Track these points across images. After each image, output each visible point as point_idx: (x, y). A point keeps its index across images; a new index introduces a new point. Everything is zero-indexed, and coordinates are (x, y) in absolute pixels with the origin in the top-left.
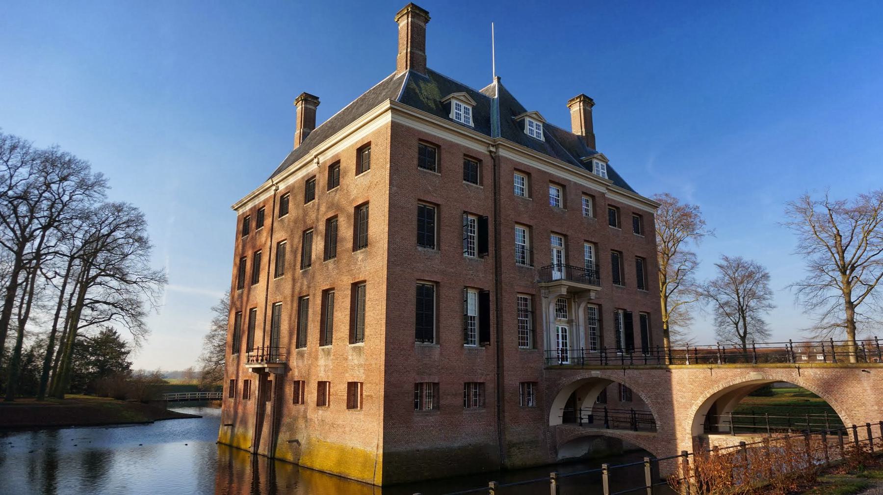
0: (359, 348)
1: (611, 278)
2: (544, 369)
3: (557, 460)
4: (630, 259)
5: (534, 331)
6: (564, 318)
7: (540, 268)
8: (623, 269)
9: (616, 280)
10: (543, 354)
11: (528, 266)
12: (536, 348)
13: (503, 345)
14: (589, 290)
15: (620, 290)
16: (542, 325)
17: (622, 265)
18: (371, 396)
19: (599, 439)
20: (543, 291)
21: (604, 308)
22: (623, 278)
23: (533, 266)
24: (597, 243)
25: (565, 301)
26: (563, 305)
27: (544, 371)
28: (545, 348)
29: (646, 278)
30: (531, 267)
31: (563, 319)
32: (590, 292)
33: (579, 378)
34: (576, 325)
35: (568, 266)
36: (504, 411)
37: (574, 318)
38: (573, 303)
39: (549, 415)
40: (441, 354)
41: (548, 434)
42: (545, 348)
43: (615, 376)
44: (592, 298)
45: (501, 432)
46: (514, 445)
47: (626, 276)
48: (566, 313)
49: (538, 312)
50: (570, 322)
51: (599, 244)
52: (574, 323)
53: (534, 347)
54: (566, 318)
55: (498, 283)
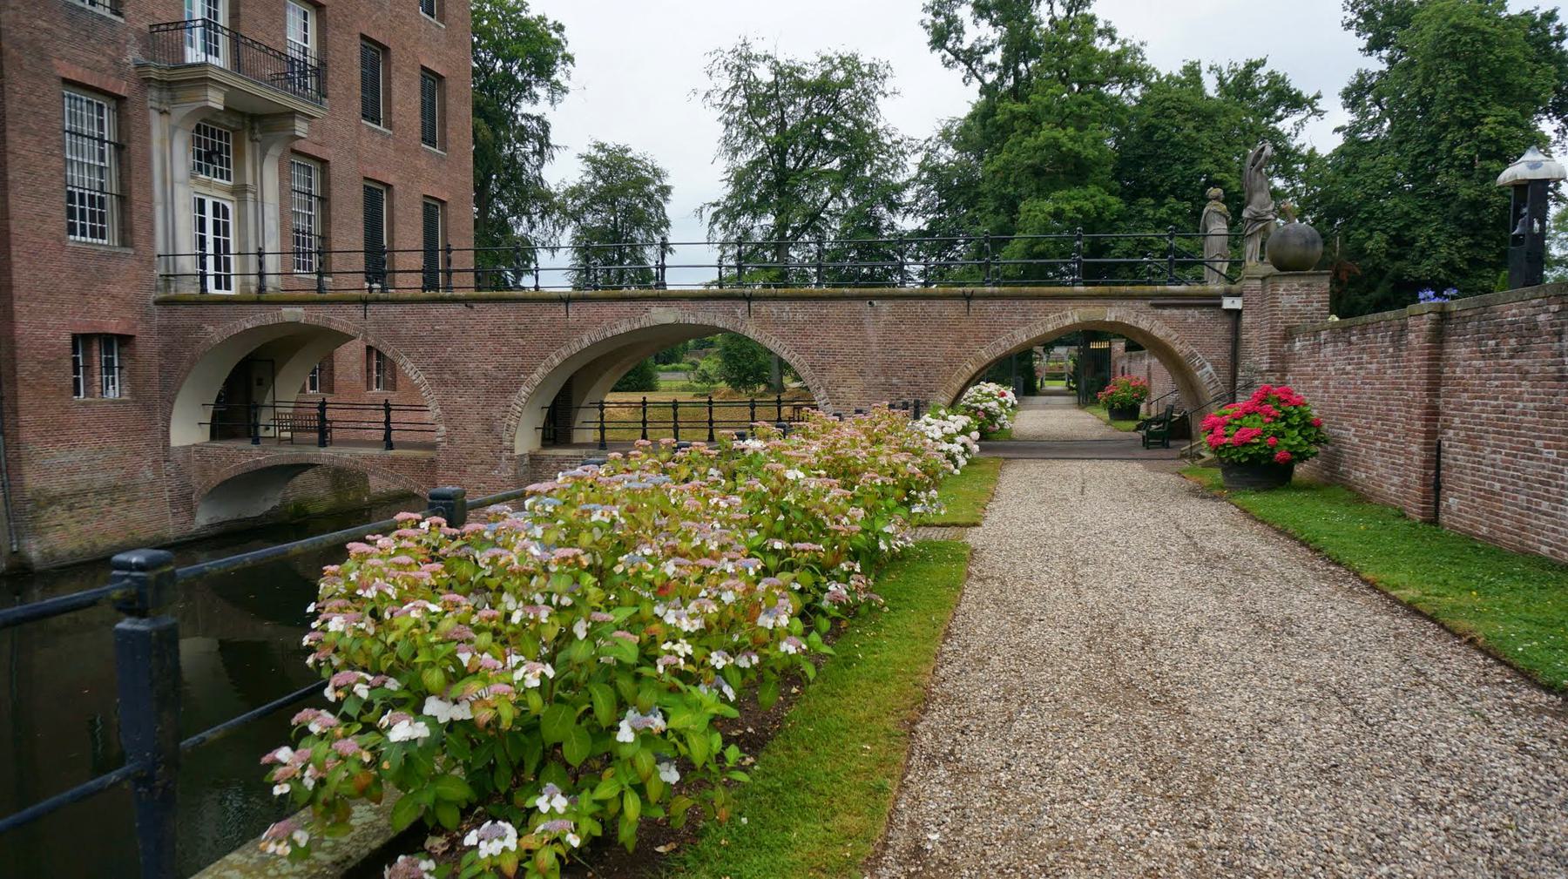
1: (357, 104)
2: (157, 303)
3: (194, 528)
4: (407, 70)
5: (123, 199)
6: (222, 178)
7: (144, 25)
8: (388, 92)
9: (371, 112)
10: (151, 262)
11: (107, 13)
12: (132, 246)
13: (8, 225)
14: (292, 114)
15: (378, 138)
16: (148, 186)
17: (388, 79)
19: (310, 473)
21: (335, 171)
22: (389, 113)
23: (120, 14)
24: (324, 6)
25: (227, 134)
26: (213, 143)
27: (156, 309)
28: (160, 248)
29: (443, 126)
30: (114, 17)
31: (218, 180)
32: (294, 118)
33: (249, 326)
34: (256, 200)
35: (236, 38)
37: (249, 181)
38: (248, 146)
39: (168, 421)
41: (170, 467)
43: (343, 319)
44: (297, 133)
46: (53, 501)
47: (396, 108)
48: (228, 166)
49: (135, 146)
50: (239, 191)
51: (328, 9)
52: (250, 196)
53: (124, 242)
54: (228, 179)
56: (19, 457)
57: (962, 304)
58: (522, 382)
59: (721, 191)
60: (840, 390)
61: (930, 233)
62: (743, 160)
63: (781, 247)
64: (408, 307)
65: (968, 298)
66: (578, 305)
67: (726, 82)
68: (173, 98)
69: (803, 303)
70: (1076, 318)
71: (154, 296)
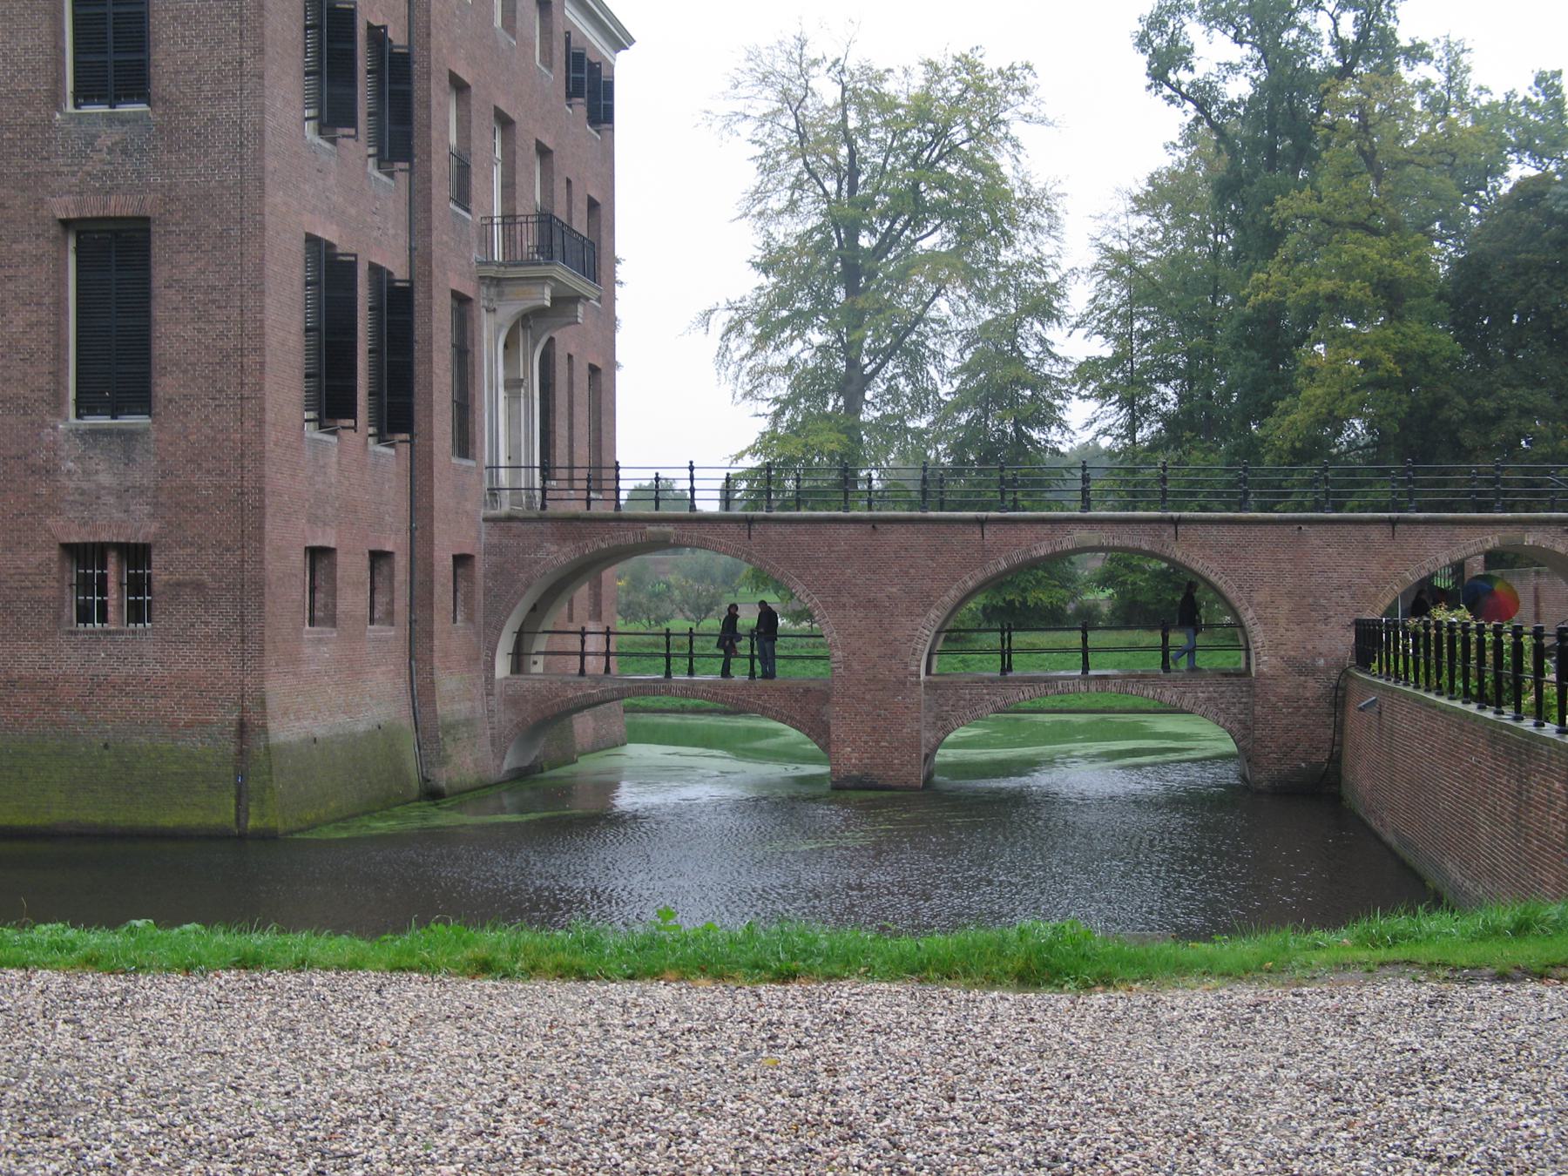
0: (128, 436)
2: (486, 520)
10: (481, 474)
12: (474, 459)
14: (576, 298)
18: (199, 586)
20: (484, 289)
23: (468, 210)
27: (483, 525)
33: (604, 546)
34: (526, 396)
36: (430, 635)
40: (339, 463)
42: (486, 462)
45: (420, 693)
55: (419, 254)
56: (432, 682)
57: (1387, 529)
58: (931, 605)
59: (749, 284)
60: (1269, 610)
61: (1114, 362)
62: (787, 230)
63: (853, 385)
64: (801, 527)
65: (1393, 522)
66: (994, 528)
67: (767, 101)
68: (500, 295)
69: (1231, 527)
70: (1497, 541)
71: (483, 512)
